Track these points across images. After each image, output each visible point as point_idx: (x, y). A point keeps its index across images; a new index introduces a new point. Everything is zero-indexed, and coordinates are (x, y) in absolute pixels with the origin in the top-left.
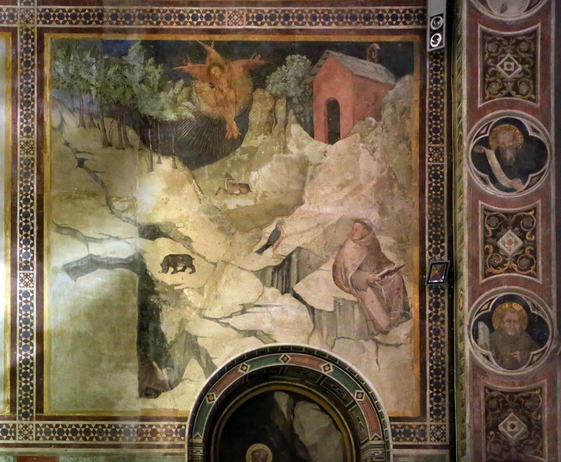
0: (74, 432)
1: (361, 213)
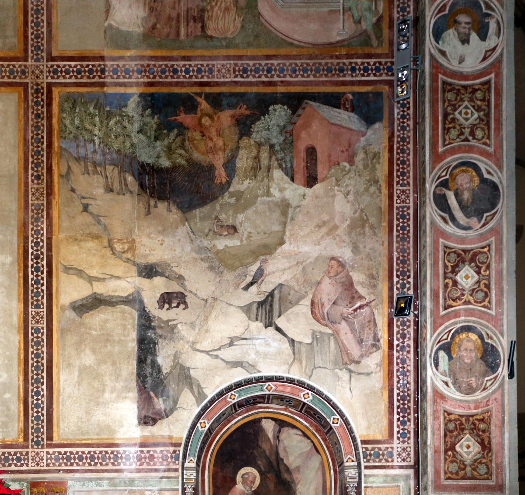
0: (81, 458)
1: (337, 252)
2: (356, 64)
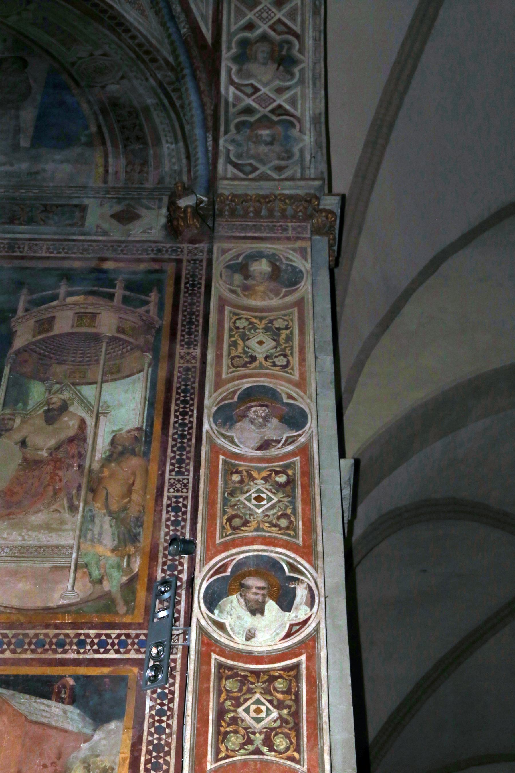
2: (88, 636)
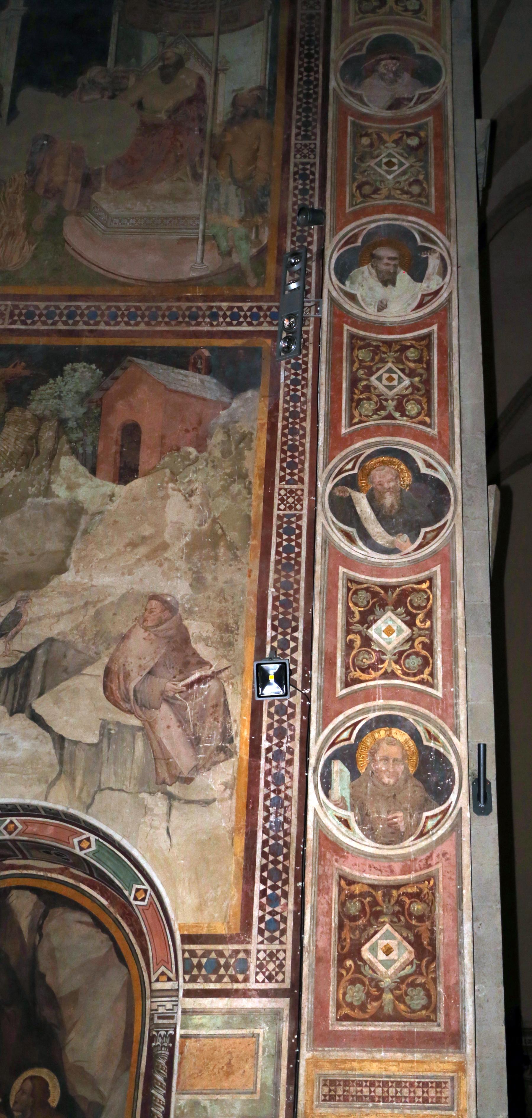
2: (220, 308)
